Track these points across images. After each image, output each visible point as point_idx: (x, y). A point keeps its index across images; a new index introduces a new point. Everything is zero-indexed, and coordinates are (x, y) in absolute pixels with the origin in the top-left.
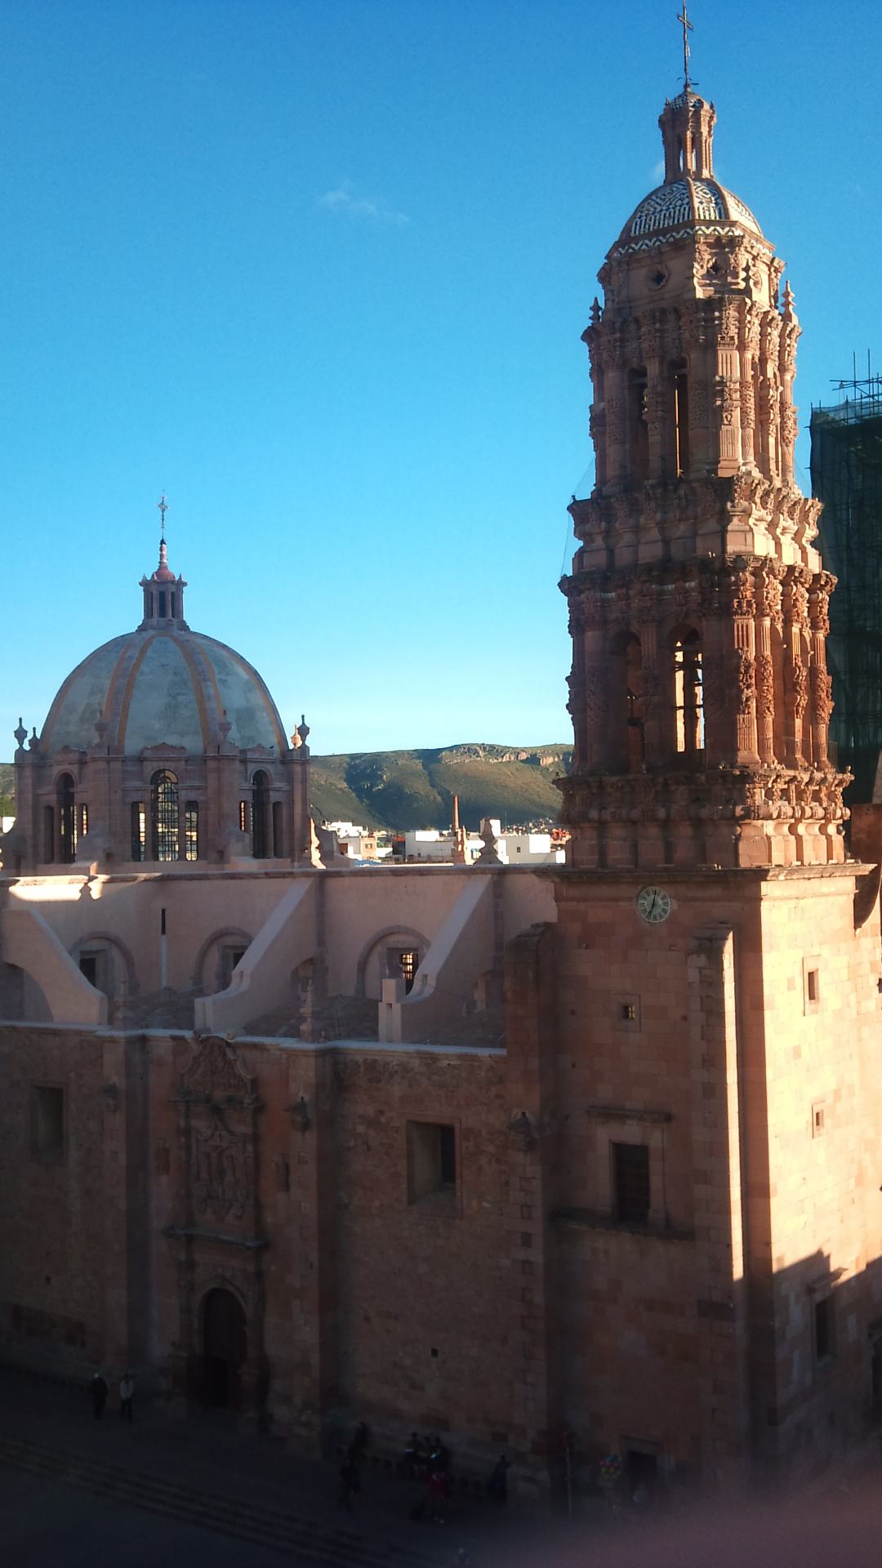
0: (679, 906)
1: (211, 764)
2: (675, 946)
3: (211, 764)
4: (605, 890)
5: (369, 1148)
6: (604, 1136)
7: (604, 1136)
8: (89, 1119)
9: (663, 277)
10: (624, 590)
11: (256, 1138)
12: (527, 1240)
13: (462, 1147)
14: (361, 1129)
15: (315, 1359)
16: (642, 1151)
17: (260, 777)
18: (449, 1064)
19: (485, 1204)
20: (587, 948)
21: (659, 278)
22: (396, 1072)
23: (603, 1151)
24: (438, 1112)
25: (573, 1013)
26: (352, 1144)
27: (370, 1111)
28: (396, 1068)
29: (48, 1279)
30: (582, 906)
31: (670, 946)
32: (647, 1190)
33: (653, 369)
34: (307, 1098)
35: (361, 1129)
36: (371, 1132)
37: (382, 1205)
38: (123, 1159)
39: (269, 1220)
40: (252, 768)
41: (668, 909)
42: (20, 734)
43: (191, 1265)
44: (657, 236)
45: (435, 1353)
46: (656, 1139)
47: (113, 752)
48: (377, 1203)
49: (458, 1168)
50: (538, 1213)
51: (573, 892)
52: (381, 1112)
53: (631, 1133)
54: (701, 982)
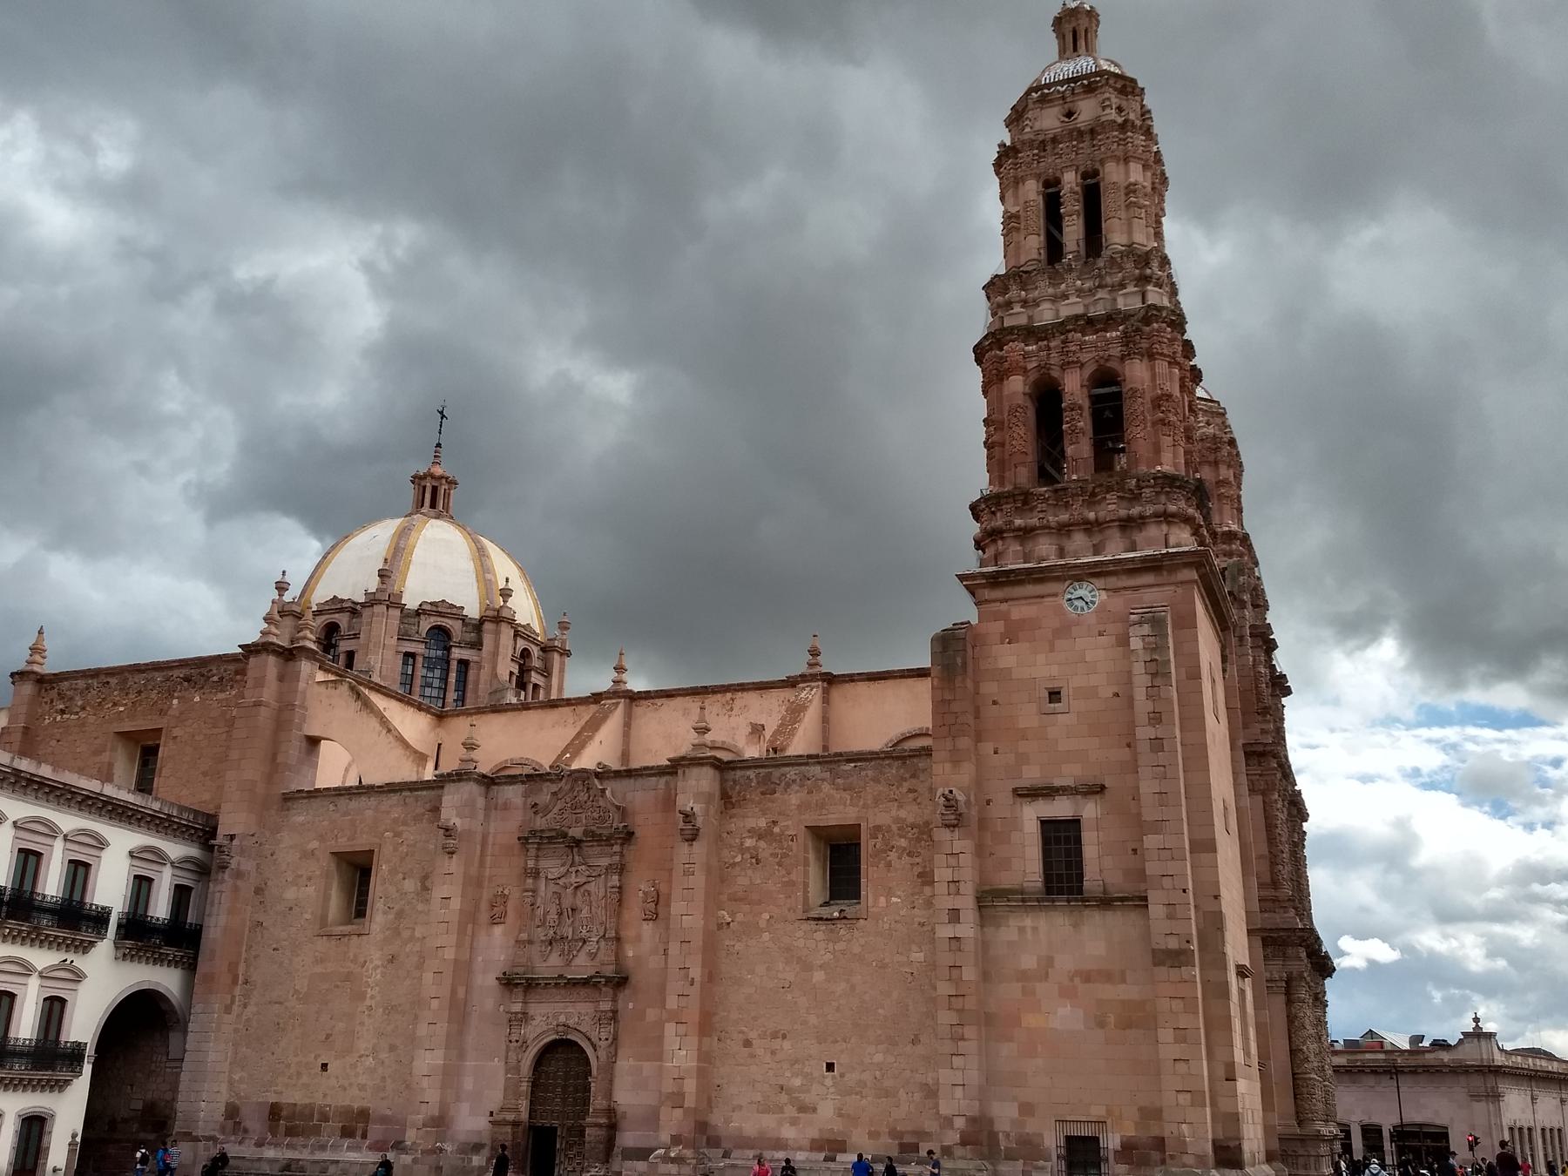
0: (1108, 596)
3: (488, 626)
4: (1030, 589)
6: (1031, 815)
7: (1031, 815)
8: (404, 879)
10: (1045, 343)
11: (621, 869)
12: (954, 916)
13: (867, 846)
14: (749, 843)
15: (690, 1086)
16: (1075, 823)
17: (525, 654)
18: (855, 766)
19: (894, 900)
20: (1009, 643)
21: (1069, 114)
22: (794, 781)
23: (1031, 828)
24: (839, 813)
25: (995, 703)
26: (738, 859)
27: (762, 823)
29: (324, 1067)
30: (1004, 606)
32: (1079, 864)
33: (1070, 180)
35: (749, 843)
36: (762, 844)
38: (456, 904)
39: (630, 954)
40: (521, 644)
41: (1096, 600)
42: (281, 587)
43: (524, 1017)
44: (1068, 83)
45: (830, 1067)
47: (394, 602)
49: (863, 867)
50: (968, 889)
52: (775, 823)
53: (1061, 809)
54: (1144, 648)
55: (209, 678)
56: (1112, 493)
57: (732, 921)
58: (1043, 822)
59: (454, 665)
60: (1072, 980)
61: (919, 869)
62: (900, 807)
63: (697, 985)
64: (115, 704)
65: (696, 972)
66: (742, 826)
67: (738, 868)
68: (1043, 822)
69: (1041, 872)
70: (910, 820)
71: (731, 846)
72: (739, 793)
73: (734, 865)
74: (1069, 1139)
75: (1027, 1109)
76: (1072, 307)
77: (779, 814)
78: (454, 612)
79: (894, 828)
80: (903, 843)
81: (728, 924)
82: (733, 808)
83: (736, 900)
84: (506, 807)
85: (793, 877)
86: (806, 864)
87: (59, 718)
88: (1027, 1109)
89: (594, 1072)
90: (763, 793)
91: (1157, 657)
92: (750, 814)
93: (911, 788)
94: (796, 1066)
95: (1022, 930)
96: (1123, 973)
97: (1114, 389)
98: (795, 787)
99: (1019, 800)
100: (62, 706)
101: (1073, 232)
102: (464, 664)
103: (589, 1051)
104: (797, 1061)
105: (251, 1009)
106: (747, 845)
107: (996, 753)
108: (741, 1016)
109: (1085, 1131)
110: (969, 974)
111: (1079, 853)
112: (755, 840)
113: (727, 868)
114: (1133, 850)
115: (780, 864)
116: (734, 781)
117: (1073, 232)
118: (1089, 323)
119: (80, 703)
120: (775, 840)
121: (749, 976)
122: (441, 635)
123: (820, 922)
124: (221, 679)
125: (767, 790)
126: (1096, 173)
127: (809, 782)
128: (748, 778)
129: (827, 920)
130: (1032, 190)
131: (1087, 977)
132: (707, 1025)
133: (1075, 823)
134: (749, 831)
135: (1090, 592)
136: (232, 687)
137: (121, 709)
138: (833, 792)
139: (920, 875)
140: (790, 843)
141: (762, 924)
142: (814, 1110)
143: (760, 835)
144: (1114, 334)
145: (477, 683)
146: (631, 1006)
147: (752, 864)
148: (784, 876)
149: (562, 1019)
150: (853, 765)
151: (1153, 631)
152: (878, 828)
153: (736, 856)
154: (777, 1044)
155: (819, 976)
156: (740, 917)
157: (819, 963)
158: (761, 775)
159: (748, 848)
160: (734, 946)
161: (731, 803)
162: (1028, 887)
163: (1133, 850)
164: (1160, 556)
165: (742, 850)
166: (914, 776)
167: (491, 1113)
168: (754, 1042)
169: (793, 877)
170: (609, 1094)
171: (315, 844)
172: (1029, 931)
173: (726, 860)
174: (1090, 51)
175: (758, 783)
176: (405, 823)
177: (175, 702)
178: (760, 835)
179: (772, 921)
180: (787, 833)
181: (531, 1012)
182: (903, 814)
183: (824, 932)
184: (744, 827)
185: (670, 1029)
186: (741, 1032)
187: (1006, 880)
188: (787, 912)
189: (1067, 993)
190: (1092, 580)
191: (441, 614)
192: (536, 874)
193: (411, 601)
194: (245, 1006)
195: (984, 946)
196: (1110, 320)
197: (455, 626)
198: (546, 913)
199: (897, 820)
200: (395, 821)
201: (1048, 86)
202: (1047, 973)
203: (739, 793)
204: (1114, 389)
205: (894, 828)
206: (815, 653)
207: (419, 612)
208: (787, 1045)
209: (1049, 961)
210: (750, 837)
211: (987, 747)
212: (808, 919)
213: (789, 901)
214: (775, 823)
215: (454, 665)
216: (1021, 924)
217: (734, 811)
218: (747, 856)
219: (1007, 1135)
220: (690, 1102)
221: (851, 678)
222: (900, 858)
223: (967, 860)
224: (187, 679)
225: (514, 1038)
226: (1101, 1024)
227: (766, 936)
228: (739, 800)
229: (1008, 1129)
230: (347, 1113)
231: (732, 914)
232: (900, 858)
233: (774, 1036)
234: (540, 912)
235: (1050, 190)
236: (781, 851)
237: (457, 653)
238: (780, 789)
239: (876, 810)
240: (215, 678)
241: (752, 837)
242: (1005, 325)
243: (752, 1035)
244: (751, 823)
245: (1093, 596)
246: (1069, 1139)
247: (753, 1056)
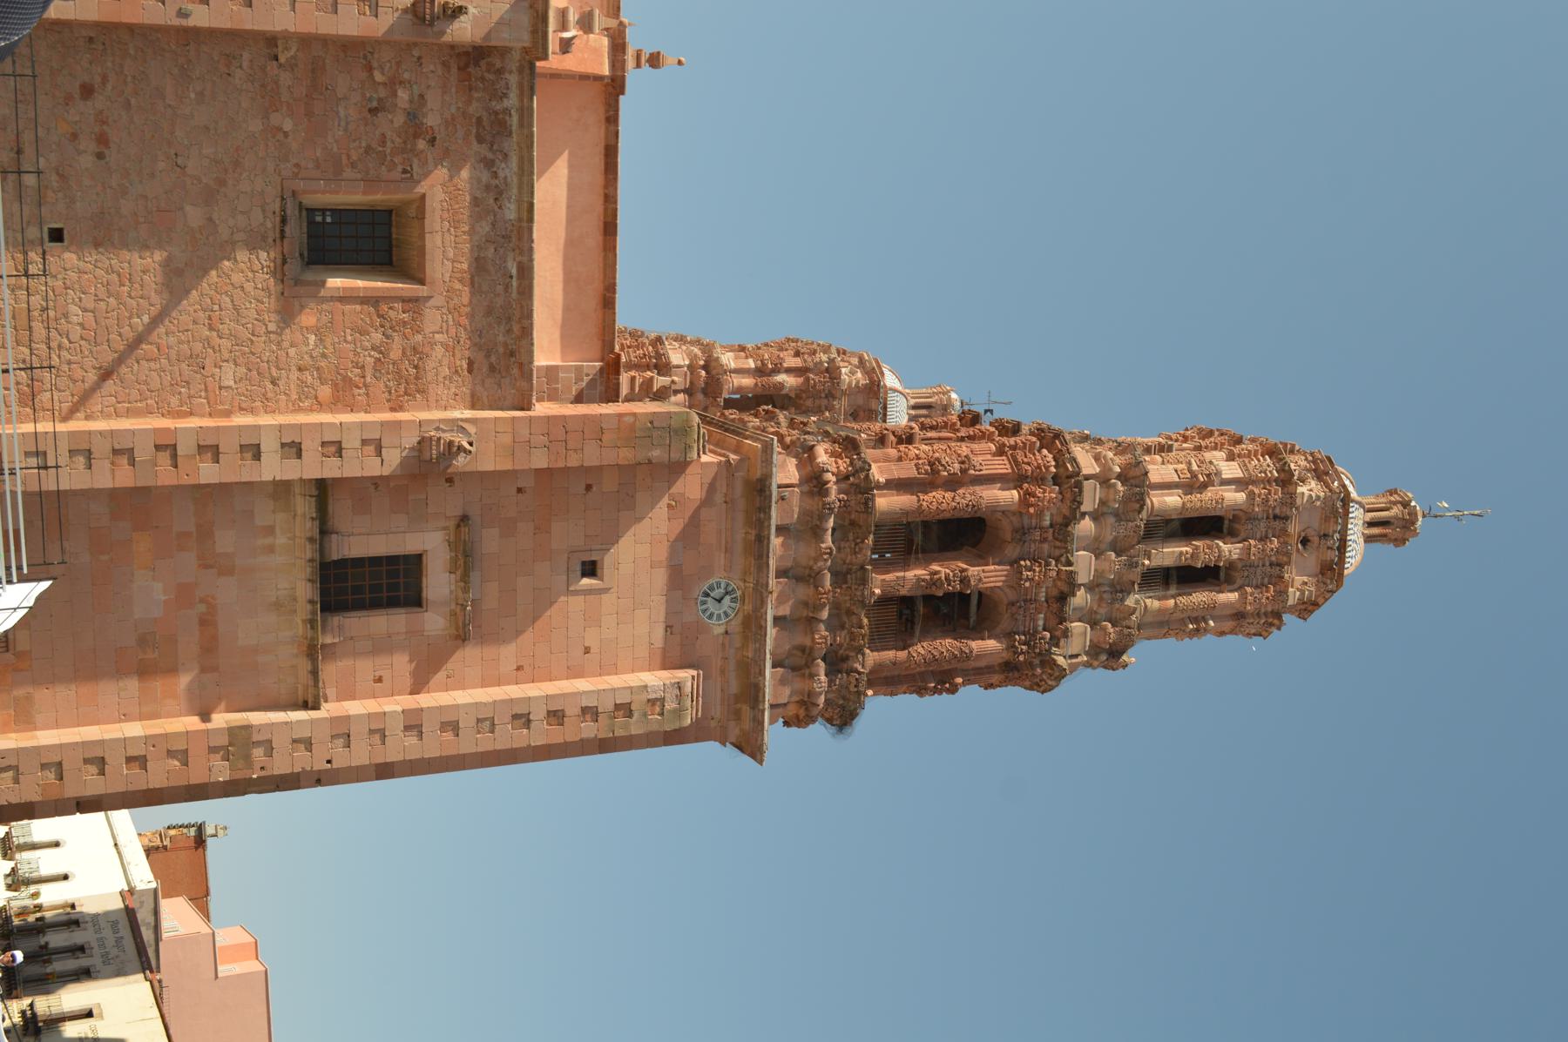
0: (718, 635)
2: (671, 633)
5: (373, 111)
6: (431, 543)
7: (431, 543)
9: (1301, 542)
14: (403, 95)
16: (414, 600)
18: (511, 277)
23: (408, 544)
25: (589, 487)
26: (378, 77)
27: (432, 120)
28: (501, 174)
31: (671, 627)
36: (399, 120)
37: (286, 134)
46: (434, 622)
48: (288, 125)
50: (331, 469)
51: (739, 489)
52: (432, 141)
53: (438, 582)
56: (847, 637)
57: (280, 66)
58: (418, 558)
60: (202, 601)
66: (433, 84)
67: (364, 75)
68: (418, 558)
69: (351, 557)
71: (398, 64)
72: (483, 79)
73: (370, 69)
80: (395, 354)
82: (459, 69)
83: (313, 71)
90: (479, 120)
91: (634, 718)
92: (447, 98)
93: (475, 366)
94: (54, 177)
95: (270, 531)
96: (215, 669)
98: (485, 176)
99: (452, 524)
101: (1171, 553)
104: (62, 177)
106: (400, 93)
107: (520, 490)
108: (129, 79)
110: (208, 473)
111: (375, 604)
112: (407, 106)
113: (365, 57)
114: (381, 677)
115: (368, 150)
116: (500, 72)
117: (1171, 553)
120: (405, 142)
121: (193, 95)
123: (278, 219)
125: (484, 127)
127: (492, 201)
128: (505, 95)
129: (282, 231)
131: (206, 622)
133: (414, 600)
134: (421, 96)
135: (725, 613)
140: (400, 168)
141: (275, 119)
143: (413, 116)
144: (1041, 623)
147: (370, 100)
148: (349, 157)
150: (514, 272)
151: (669, 711)
153: (383, 74)
154: (88, 144)
155: (194, 215)
156: (285, 78)
157: (215, 216)
158: (507, 118)
159: (395, 94)
160: (241, 67)
161: (467, 65)
162: (331, 542)
163: (381, 677)
164: (761, 707)
165: (393, 83)
166: (492, 369)
168: (89, 103)
172: (268, 541)
173: (376, 56)
175: (496, 113)
178: (413, 116)
179: (280, 136)
180: (416, 161)
183: (262, 224)
184: (429, 87)
186: (105, 79)
187: (340, 511)
188: (295, 161)
189: (184, 594)
190: (740, 615)
202: (211, 567)
203: (483, 79)
206: (655, 60)
208: (87, 161)
209: (227, 571)
210: (412, 95)
212: (283, 199)
213: (311, 165)
214: (432, 141)
216: (278, 531)
217: (454, 70)
218: (382, 93)
221: (612, 119)
223: (373, 467)
226: (143, 641)
227: (256, 126)
228: (470, 80)
231: (291, 66)
233: (102, 140)
236: (388, 151)
238: (484, 150)
239: (444, 310)
241: (411, 102)
243: (99, 101)
244: (433, 100)
245: (719, 617)
247: (68, 99)
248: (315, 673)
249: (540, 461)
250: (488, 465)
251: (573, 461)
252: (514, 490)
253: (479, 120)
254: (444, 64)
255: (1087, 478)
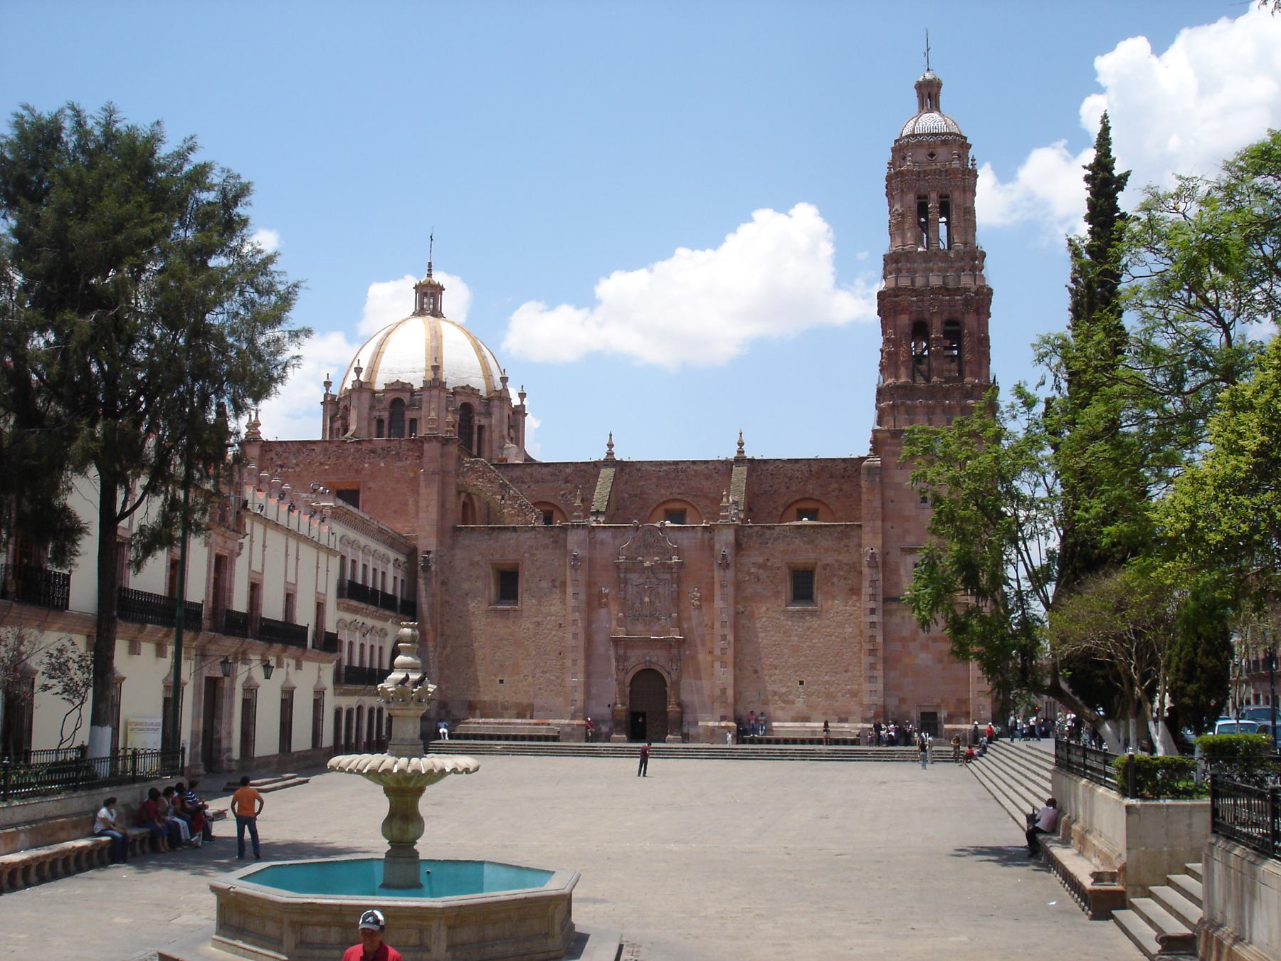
1: (496, 403)
3: (496, 403)
5: (759, 580)
14: (753, 570)
15: (730, 692)
21: (932, 155)
25: (892, 501)
26: (747, 578)
27: (761, 560)
34: (727, 552)
36: (761, 571)
39: (686, 626)
43: (626, 658)
45: (801, 683)
50: (880, 598)
52: (768, 560)
55: (388, 452)
59: (476, 429)
61: (849, 587)
62: (839, 554)
63: (732, 646)
64: (321, 464)
65: (730, 638)
70: (845, 561)
73: (745, 581)
74: (922, 713)
75: (902, 701)
76: (935, 281)
77: (772, 555)
78: (473, 392)
79: (836, 565)
81: (743, 612)
84: (602, 543)
85: (779, 588)
86: (786, 583)
87: (279, 470)
88: (902, 701)
89: (669, 684)
95: (903, 618)
97: (956, 328)
100: (280, 463)
102: (481, 428)
103: (665, 675)
105: (448, 649)
107: (892, 528)
109: (931, 710)
110: (879, 639)
115: (772, 582)
118: (945, 289)
119: (294, 461)
122: (466, 410)
124: (398, 454)
126: (947, 197)
130: (911, 198)
132: (736, 665)
136: (406, 459)
137: (327, 467)
138: (802, 545)
139: (850, 590)
142: (794, 703)
143: (762, 566)
145: (491, 441)
146: (687, 653)
149: (648, 658)
152: (828, 565)
165: (749, 574)
167: (609, 706)
169: (779, 588)
170: (678, 696)
171: (477, 558)
174: (935, 107)
176: (537, 549)
177: (366, 465)
178: (762, 566)
181: (628, 655)
182: (841, 558)
185: (717, 665)
186: (752, 666)
191: (468, 395)
192: (626, 582)
193: (450, 386)
194: (444, 648)
195: (885, 625)
196: (957, 291)
197: (475, 402)
198: (633, 604)
199: (837, 561)
200: (531, 547)
201: (920, 135)
204: (956, 328)
205: (836, 565)
207: (456, 392)
211: (888, 525)
215: (476, 429)
217: (743, 552)
218: (753, 577)
219: (893, 713)
220: (731, 700)
222: (839, 581)
224: (373, 451)
225: (621, 667)
226: (941, 661)
229: (893, 709)
230: (518, 705)
231: (744, 607)
232: (839, 581)
234: (630, 602)
235: (921, 201)
237: (477, 420)
240: (393, 453)
242: (900, 285)
244: (754, 560)
246: (922, 713)
247: (759, 677)
248: (960, 603)
249: (879, 523)
250: (880, 543)
251: (879, 510)
252: (892, 530)
253: (760, 543)
254: (743, 555)
255: (897, 283)
